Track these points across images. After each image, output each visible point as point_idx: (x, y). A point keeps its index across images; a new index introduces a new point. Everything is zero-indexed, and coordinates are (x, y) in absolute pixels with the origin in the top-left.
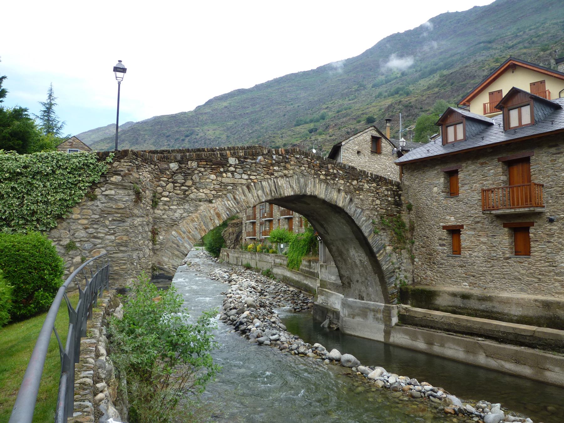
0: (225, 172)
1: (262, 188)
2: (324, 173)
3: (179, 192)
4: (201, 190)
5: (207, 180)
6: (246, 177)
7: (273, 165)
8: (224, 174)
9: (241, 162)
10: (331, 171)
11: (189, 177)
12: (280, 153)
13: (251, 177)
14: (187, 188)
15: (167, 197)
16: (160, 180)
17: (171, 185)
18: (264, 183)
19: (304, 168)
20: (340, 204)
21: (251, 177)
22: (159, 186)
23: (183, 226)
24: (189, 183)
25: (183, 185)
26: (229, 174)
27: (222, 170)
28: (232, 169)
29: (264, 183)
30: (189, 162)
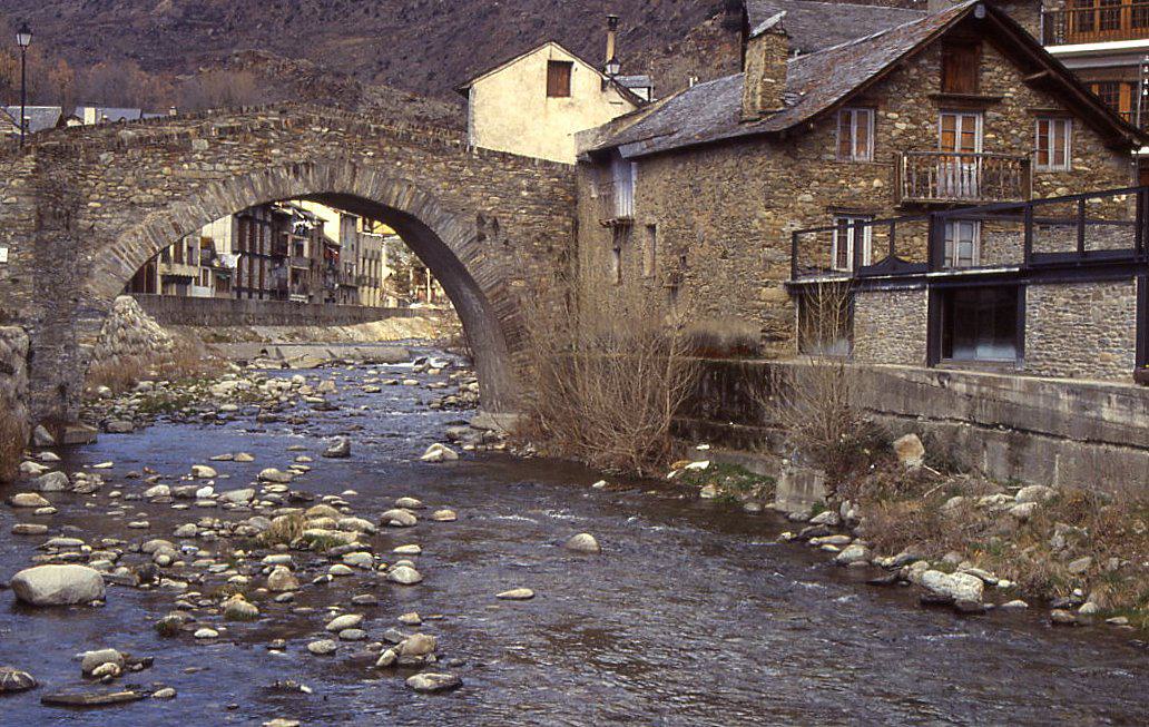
0: (186, 161)
1: (251, 185)
2: (371, 154)
3: (114, 194)
4: (148, 191)
5: (158, 176)
6: (220, 167)
7: (272, 147)
8: (186, 166)
9: (214, 144)
10: (388, 149)
11: (130, 173)
12: (284, 126)
13: (231, 168)
14: (127, 188)
15: (97, 201)
16: (86, 179)
17: (102, 184)
18: (254, 177)
19: (329, 148)
20: (404, 206)
21: (231, 168)
22: (85, 186)
23: (123, 239)
24: (129, 180)
25: (120, 183)
26: (194, 165)
27: (181, 159)
28: (199, 156)
29: (254, 177)
30: (129, 151)
